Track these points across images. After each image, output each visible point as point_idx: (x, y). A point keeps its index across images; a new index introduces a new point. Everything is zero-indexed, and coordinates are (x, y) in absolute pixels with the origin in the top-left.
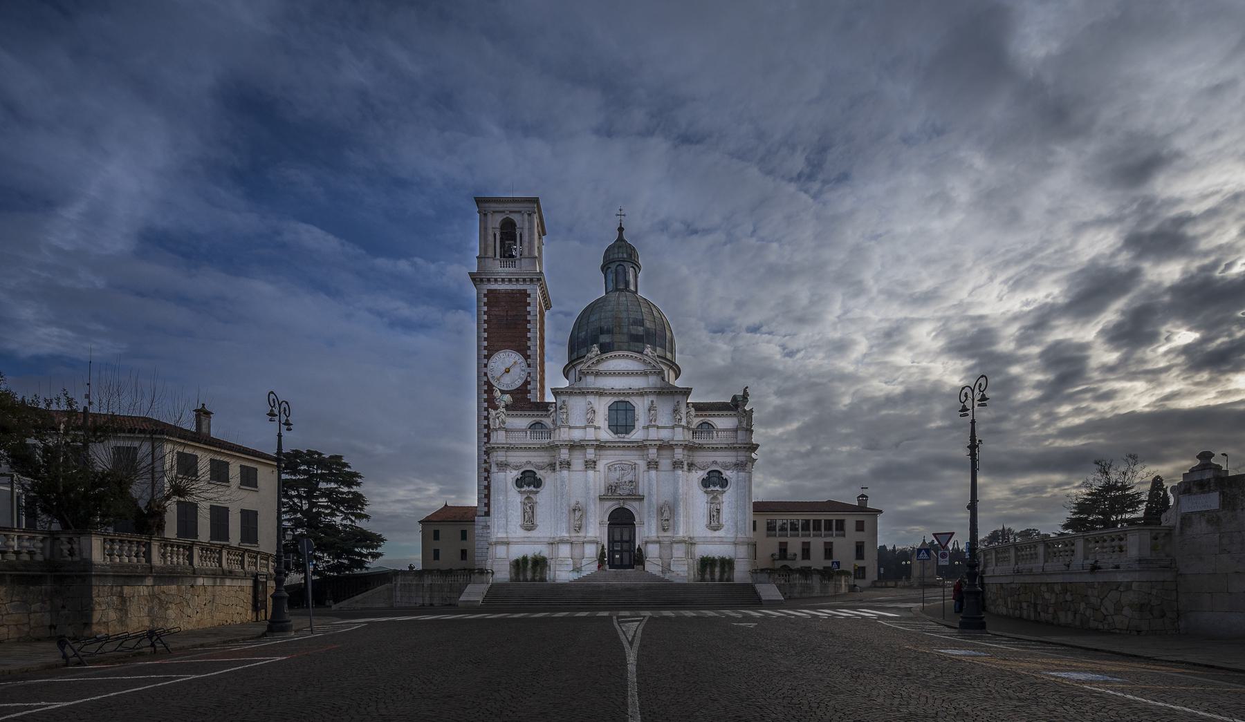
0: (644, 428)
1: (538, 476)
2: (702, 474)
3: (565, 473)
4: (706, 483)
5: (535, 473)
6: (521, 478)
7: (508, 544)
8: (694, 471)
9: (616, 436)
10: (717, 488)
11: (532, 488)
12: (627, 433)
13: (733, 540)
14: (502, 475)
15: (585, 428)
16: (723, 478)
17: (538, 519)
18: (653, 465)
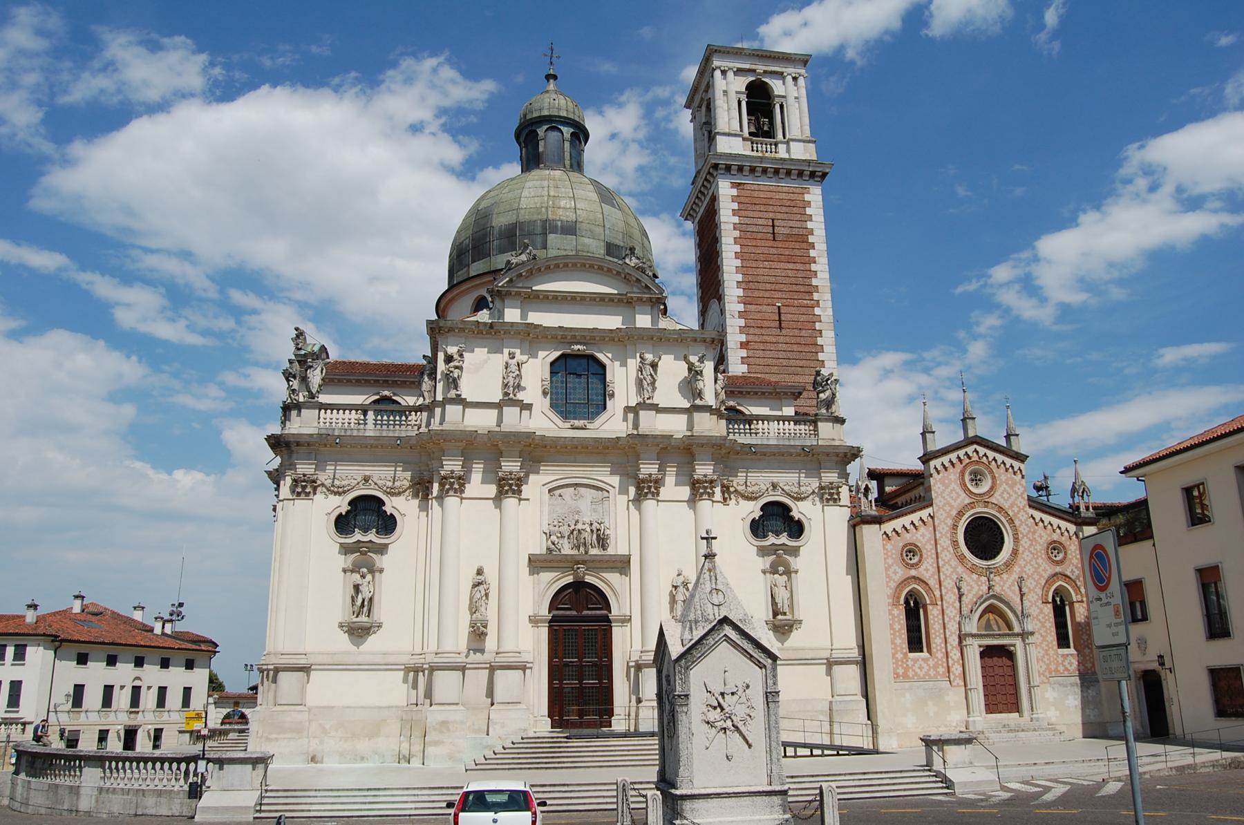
0: (628, 409)
1: (388, 509)
2: (752, 509)
3: (452, 501)
4: (758, 528)
5: (382, 503)
6: (348, 512)
7: (306, 669)
8: (733, 502)
9: (568, 425)
10: (783, 539)
11: (372, 536)
12: (592, 416)
13: (826, 654)
14: (301, 504)
15: (498, 406)
16: (792, 518)
17: (382, 612)
18: (646, 489)
